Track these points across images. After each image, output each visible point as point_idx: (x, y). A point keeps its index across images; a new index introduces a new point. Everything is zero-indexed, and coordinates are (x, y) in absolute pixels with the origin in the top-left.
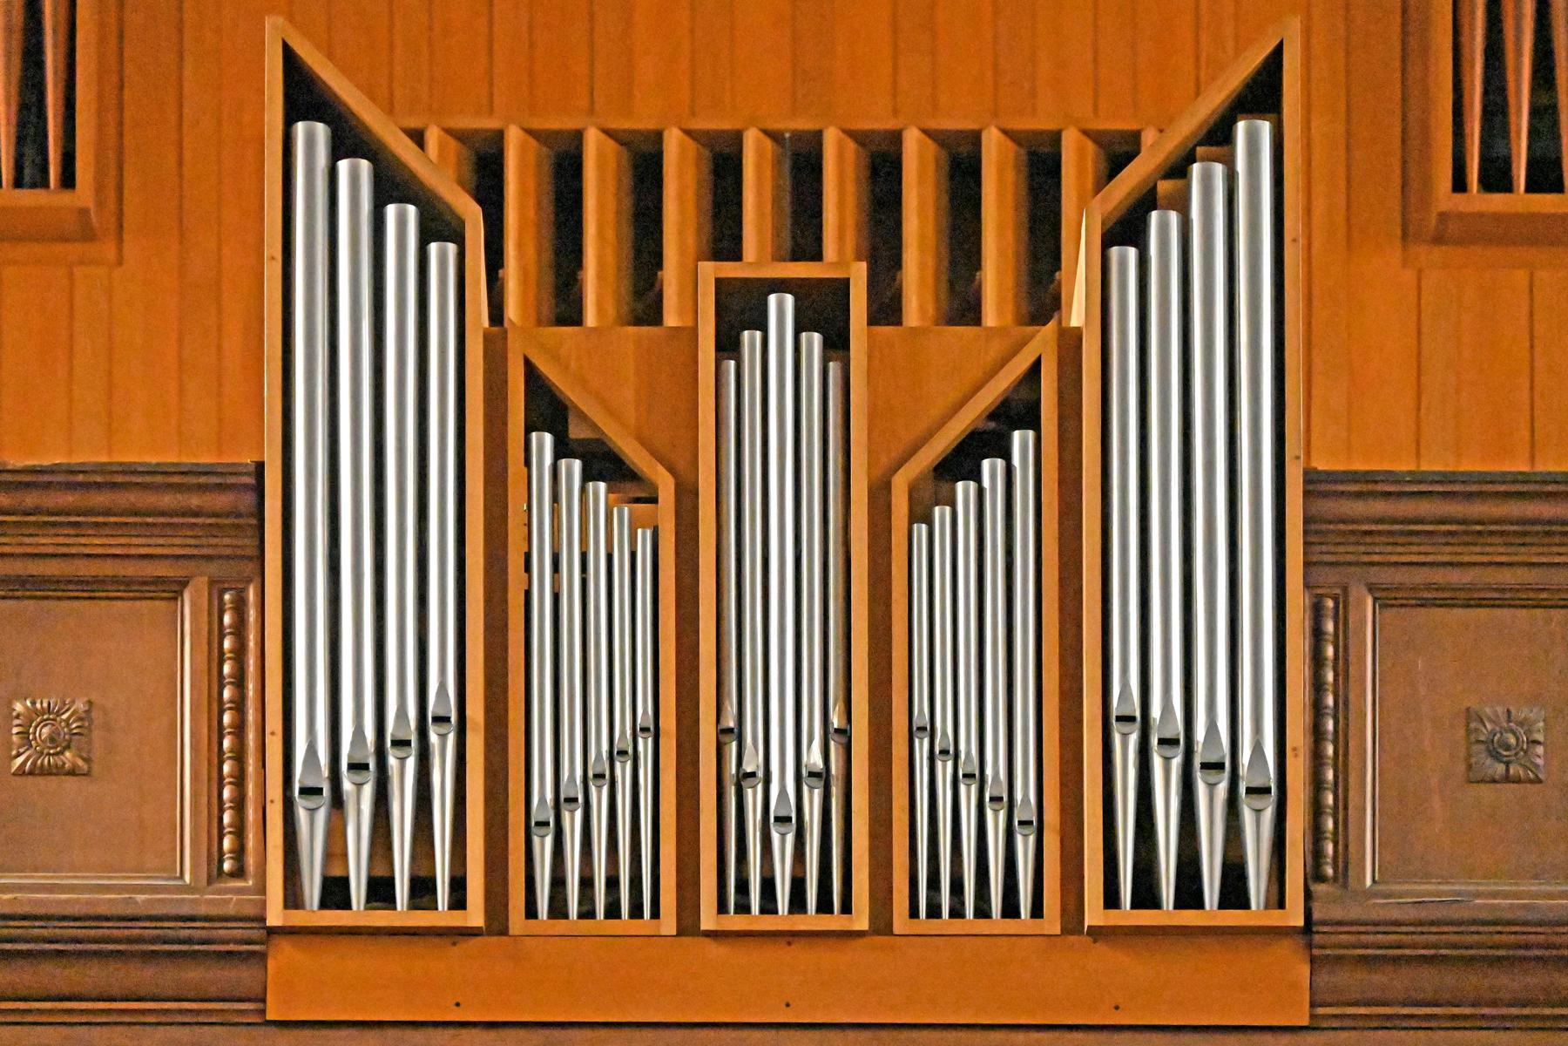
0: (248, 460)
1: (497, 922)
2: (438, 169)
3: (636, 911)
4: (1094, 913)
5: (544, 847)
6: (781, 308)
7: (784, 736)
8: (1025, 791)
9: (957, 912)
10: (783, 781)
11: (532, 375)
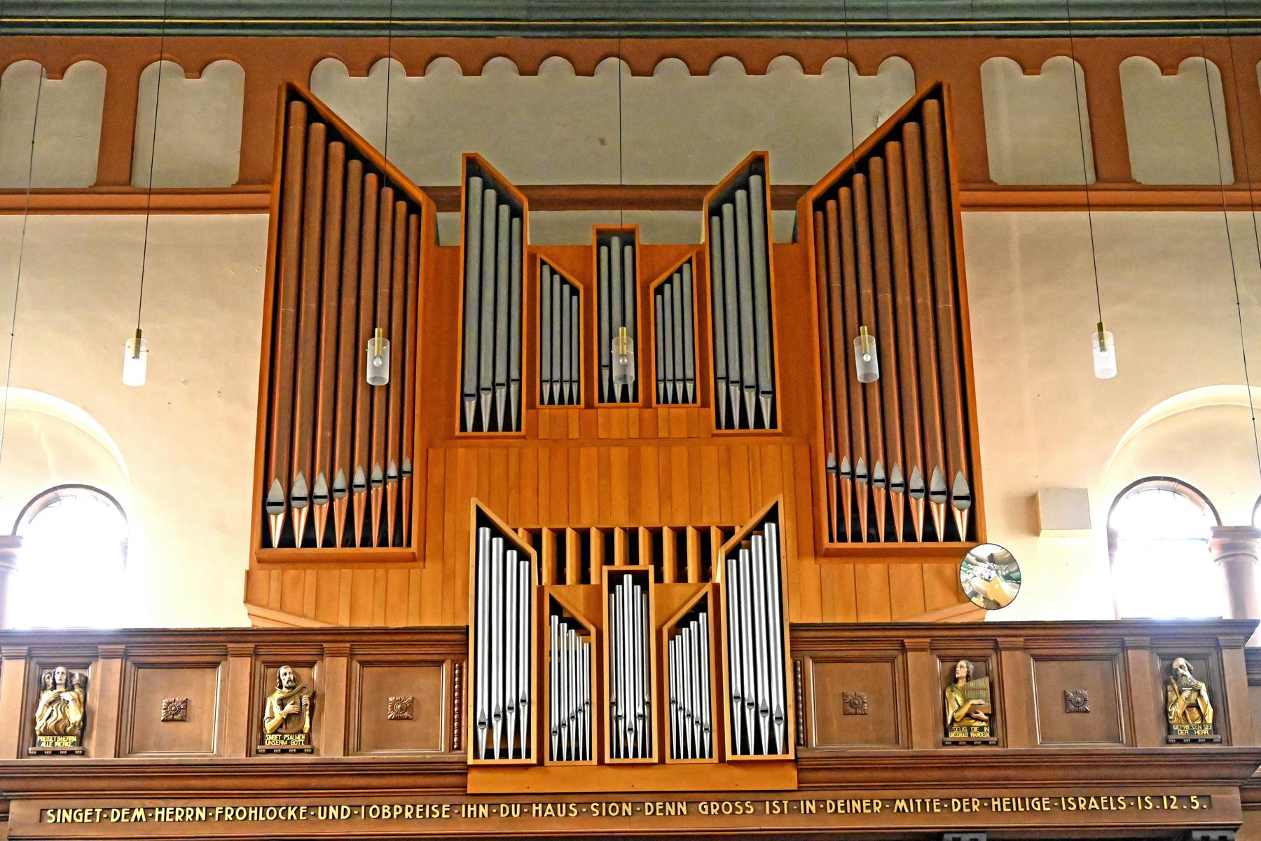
0: (462, 624)
1: (541, 762)
2: (521, 539)
3: (584, 758)
4: (729, 756)
5: (555, 739)
6: (628, 579)
7: (630, 705)
8: (706, 719)
9: (686, 756)
10: (630, 718)
11: (552, 598)
